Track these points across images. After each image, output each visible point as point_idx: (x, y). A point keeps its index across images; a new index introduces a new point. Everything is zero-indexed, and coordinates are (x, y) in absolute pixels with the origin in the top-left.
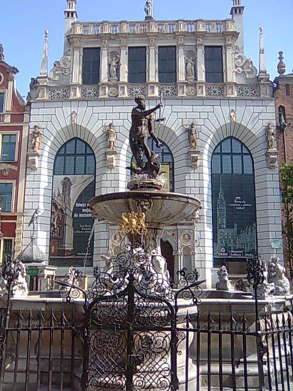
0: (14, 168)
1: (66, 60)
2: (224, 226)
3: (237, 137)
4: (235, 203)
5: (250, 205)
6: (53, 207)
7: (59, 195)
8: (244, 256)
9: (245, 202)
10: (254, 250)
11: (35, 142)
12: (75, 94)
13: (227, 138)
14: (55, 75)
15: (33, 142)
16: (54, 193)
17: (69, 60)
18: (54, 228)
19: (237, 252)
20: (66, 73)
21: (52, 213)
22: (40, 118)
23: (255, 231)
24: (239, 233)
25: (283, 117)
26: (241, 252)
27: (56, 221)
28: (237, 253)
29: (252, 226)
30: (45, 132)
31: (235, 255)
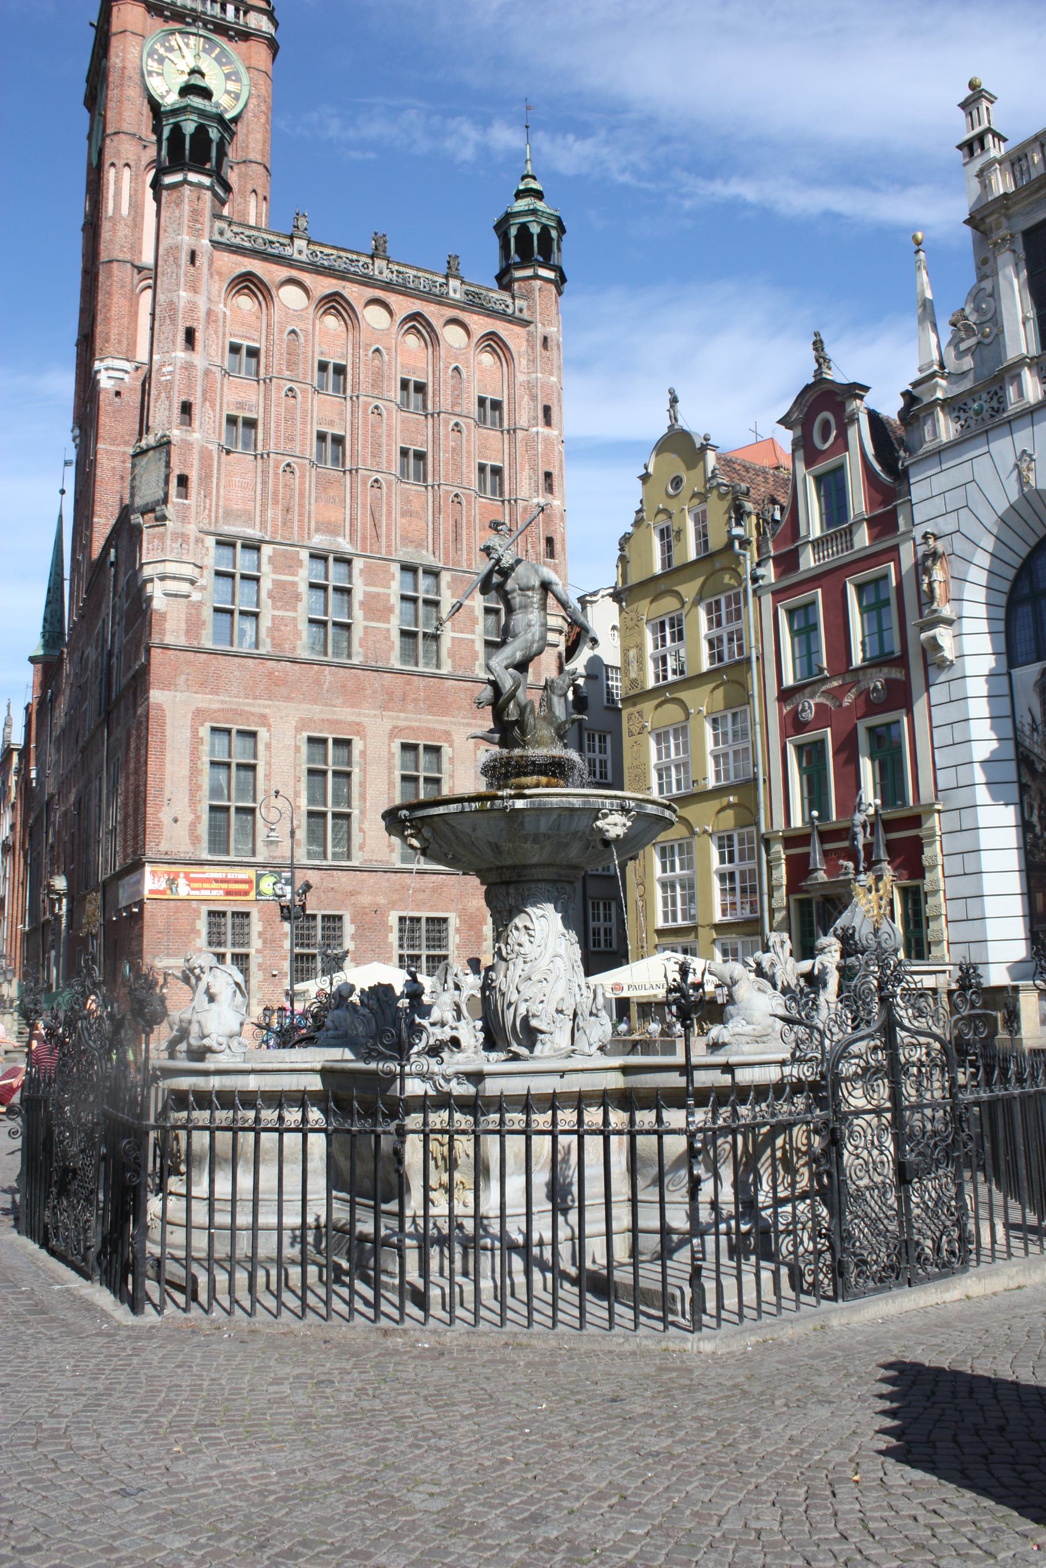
0: (896, 674)
1: (981, 294)
6: (1024, 771)
7: (1034, 729)
11: (930, 584)
12: (1021, 393)
14: (960, 355)
15: (925, 587)
16: (1019, 725)
17: (989, 290)
18: (1035, 836)
20: (988, 336)
21: (1023, 788)
22: (937, 506)
27: (1036, 812)
30: (959, 545)
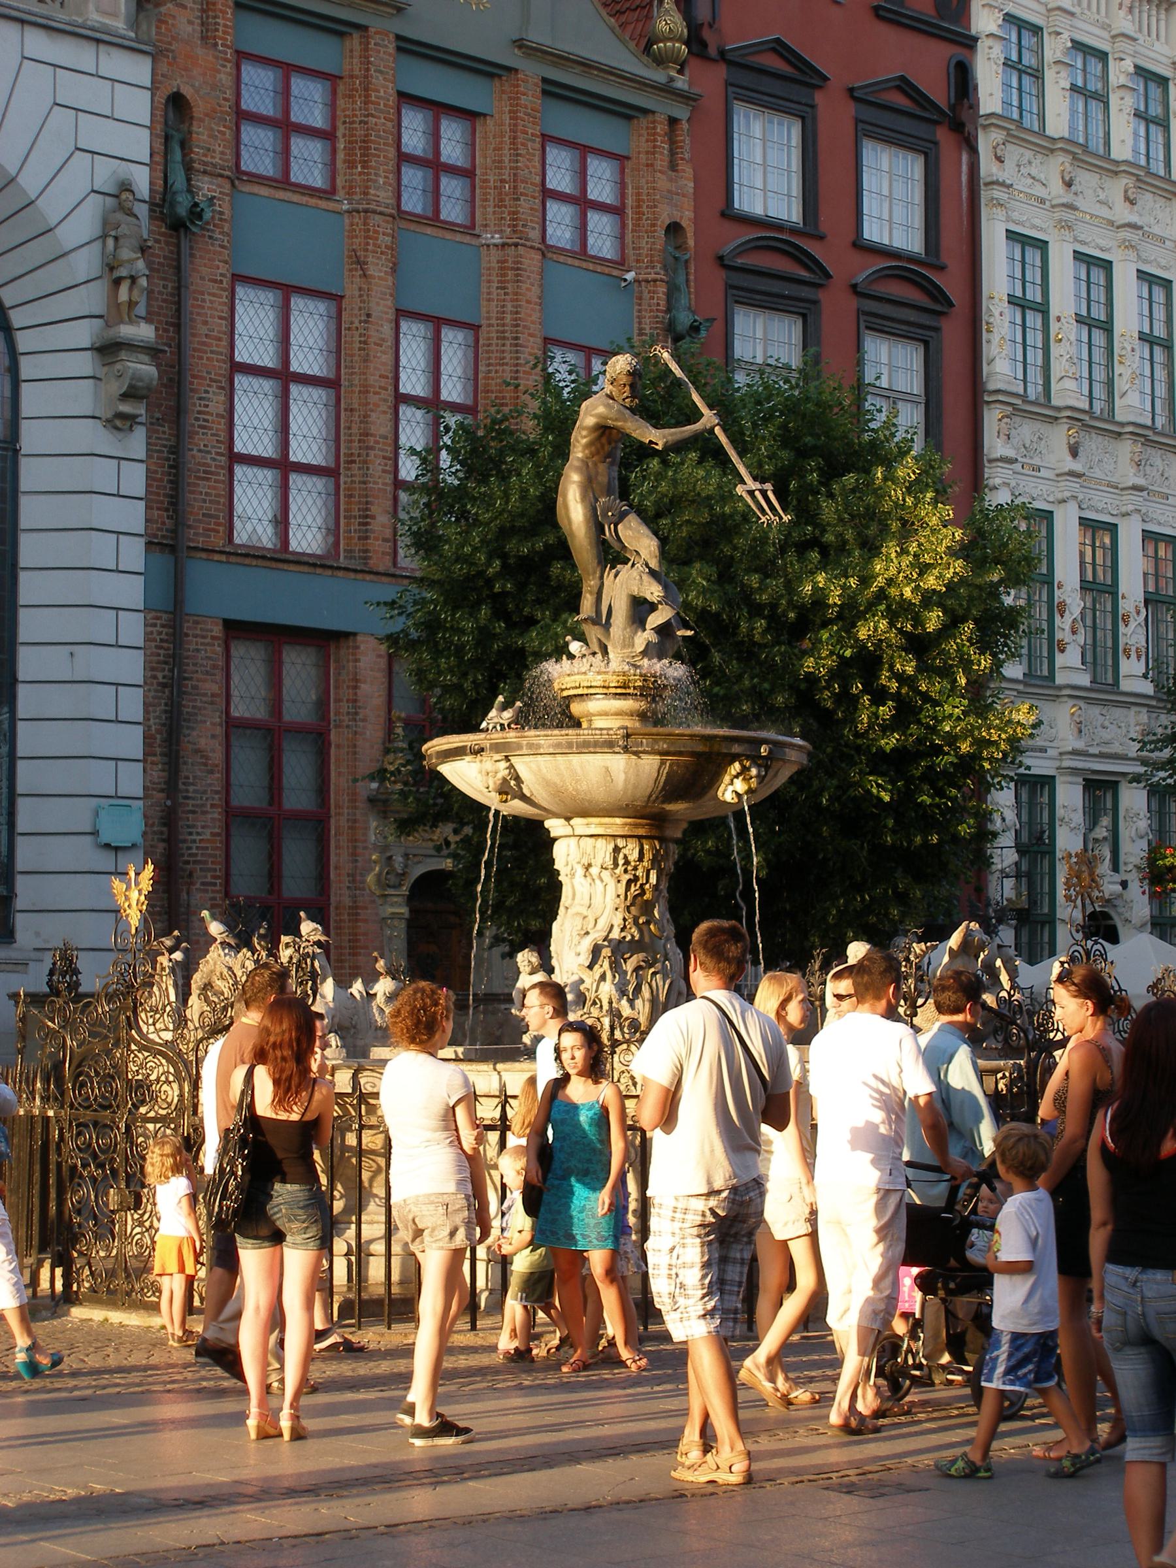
25: (178, 155)
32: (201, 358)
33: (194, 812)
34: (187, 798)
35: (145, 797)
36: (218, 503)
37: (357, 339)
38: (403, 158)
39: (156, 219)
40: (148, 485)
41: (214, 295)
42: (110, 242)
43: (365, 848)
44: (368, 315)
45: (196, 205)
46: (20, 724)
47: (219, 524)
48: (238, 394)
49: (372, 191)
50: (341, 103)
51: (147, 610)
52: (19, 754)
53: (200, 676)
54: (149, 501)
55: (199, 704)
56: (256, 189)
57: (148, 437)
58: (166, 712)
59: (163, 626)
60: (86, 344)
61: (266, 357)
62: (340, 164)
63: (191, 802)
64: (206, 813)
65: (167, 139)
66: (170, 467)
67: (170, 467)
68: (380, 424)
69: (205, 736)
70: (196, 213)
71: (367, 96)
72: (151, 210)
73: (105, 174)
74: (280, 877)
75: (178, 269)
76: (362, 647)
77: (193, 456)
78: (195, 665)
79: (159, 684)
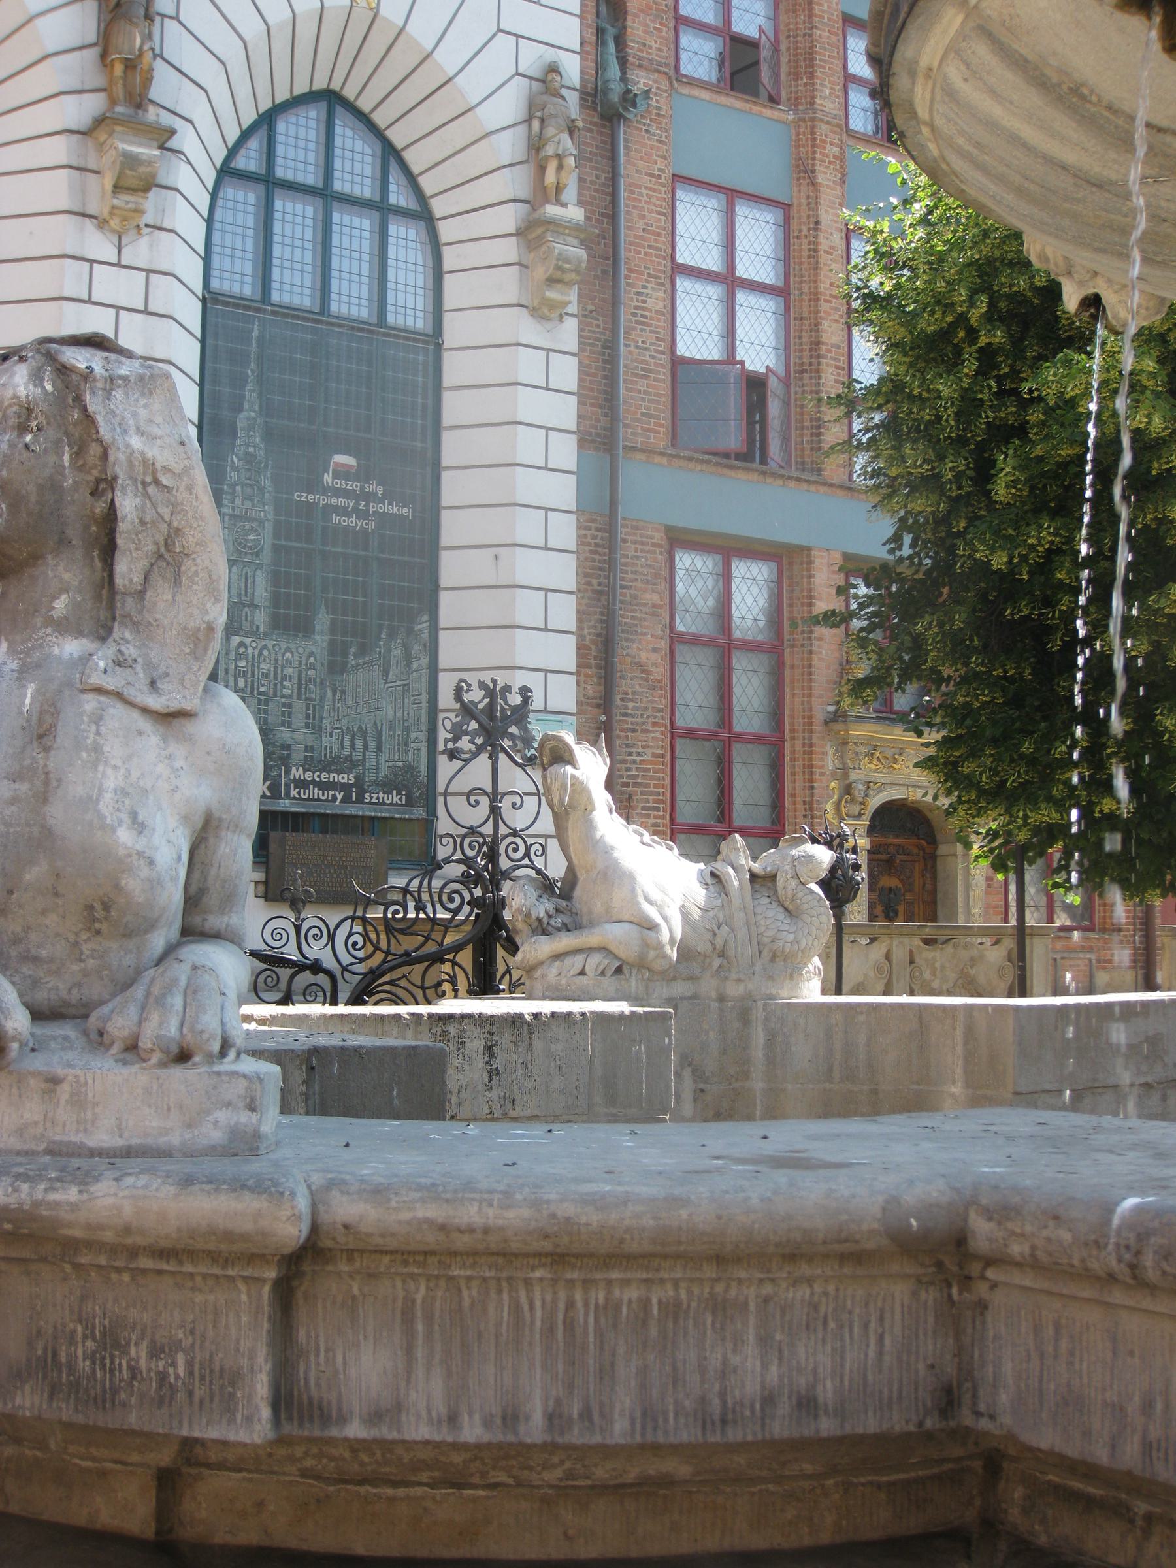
2: (261, 618)
3: (365, 104)
4: (325, 490)
5: (405, 511)
8: (360, 800)
9: (380, 489)
10: (410, 769)
13: (311, 97)
19: (324, 777)
23: (425, 661)
24: (336, 666)
25: (612, 48)
26: (343, 778)
28: (321, 786)
29: (410, 631)
31: (315, 792)
32: (639, 252)
33: (633, 730)
34: (626, 715)
35: (579, 712)
36: (658, 402)
37: (805, 247)
38: (850, 79)
39: (588, 108)
40: (580, 380)
41: (651, 189)
42: (536, 124)
43: (822, 774)
44: (817, 223)
45: (628, 91)
46: (442, 635)
47: (660, 425)
48: (680, 295)
49: (818, 101)
50: (783, 18)
51: (579, 512)
52: (441, 666)
53: (639, 584)
54: (582, 395)
55: (638, 615)
56: (696, 92)
57: (580, 330)
58: (602, 621)
59: (598, 530)
60: (512, 230)
61: (712, 261)
62: (783, 77)
63: (630, 719)
64: (648, 731)
65: (600, 32)
66: (605, 362)
67: (605, 362)
68: (831, 332)
69: (643, 649)
70: (628, 98)
71: (811, 10)
72: (581, 99)
73: (532, 58)
74: (730, 803)
75: (613, 158)
76: (817, 562)
77: (630, 353)
78: (635, 573)
79: (594, 591)
